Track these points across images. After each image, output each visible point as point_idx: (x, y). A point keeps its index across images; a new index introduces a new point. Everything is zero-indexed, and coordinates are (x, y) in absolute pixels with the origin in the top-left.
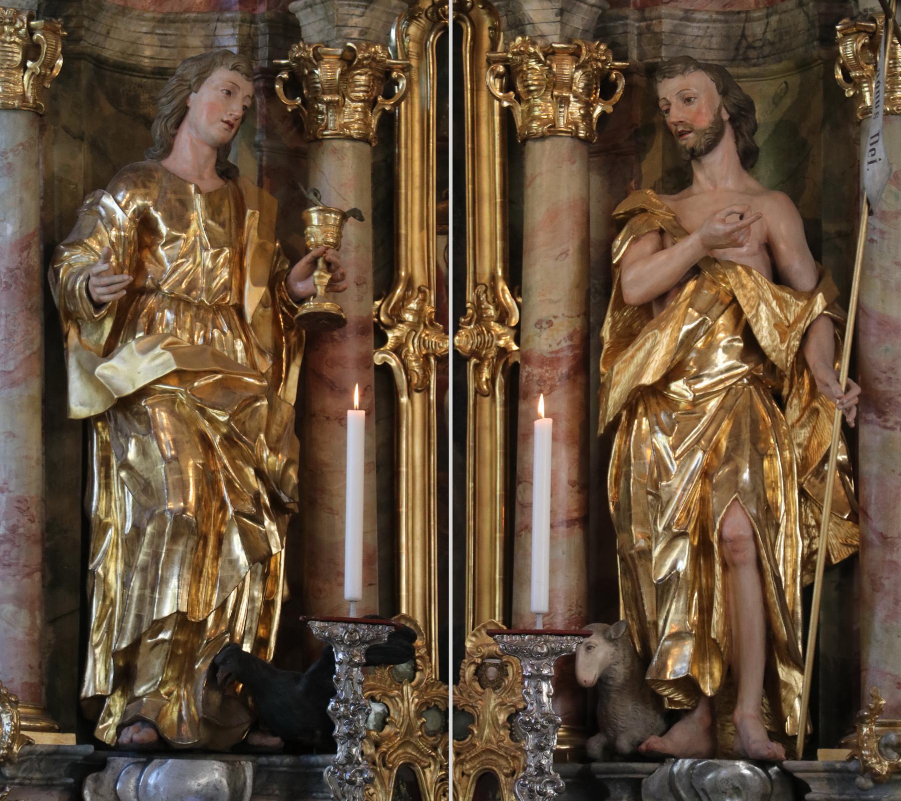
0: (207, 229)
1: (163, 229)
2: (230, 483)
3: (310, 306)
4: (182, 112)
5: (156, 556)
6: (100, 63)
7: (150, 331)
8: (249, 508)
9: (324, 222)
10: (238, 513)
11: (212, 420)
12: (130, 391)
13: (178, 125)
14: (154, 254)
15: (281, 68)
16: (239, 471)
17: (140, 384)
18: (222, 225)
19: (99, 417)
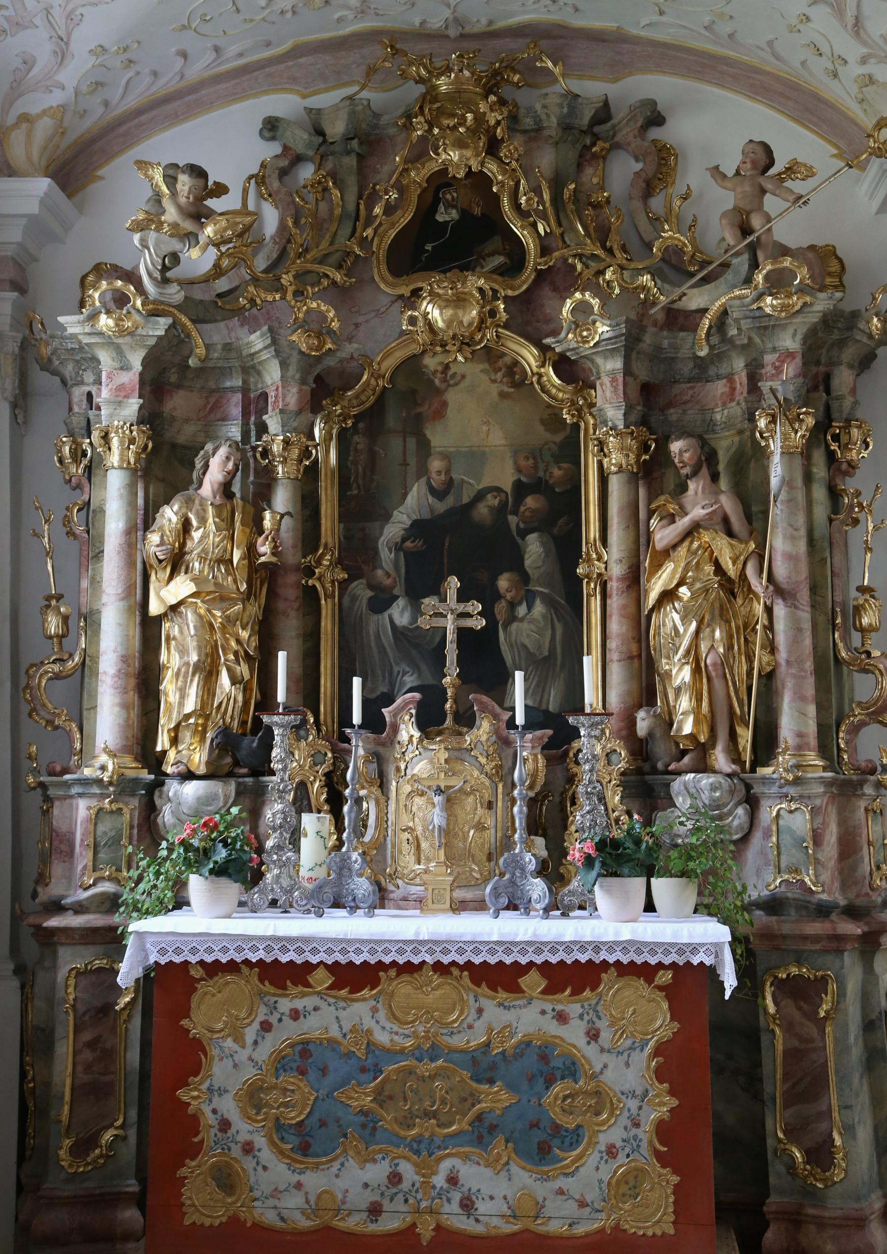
0: (215, 522)
1: (195, 523)
2: (222, 646)
3: (263, 559)
4: (206, 467)
5: (185, 682)
6: (174, 446)
7: (186, 573)
8: (232, 657)
9: (273, 518)
10: (226, 660)
11: (214, 616)
12: (174, 602)
13: (204, 474)
14: (190, 535)
15: (258, 446)
16: (227, 640)
17: (179, 599)
18: (223, 520)
19: (165, 614)
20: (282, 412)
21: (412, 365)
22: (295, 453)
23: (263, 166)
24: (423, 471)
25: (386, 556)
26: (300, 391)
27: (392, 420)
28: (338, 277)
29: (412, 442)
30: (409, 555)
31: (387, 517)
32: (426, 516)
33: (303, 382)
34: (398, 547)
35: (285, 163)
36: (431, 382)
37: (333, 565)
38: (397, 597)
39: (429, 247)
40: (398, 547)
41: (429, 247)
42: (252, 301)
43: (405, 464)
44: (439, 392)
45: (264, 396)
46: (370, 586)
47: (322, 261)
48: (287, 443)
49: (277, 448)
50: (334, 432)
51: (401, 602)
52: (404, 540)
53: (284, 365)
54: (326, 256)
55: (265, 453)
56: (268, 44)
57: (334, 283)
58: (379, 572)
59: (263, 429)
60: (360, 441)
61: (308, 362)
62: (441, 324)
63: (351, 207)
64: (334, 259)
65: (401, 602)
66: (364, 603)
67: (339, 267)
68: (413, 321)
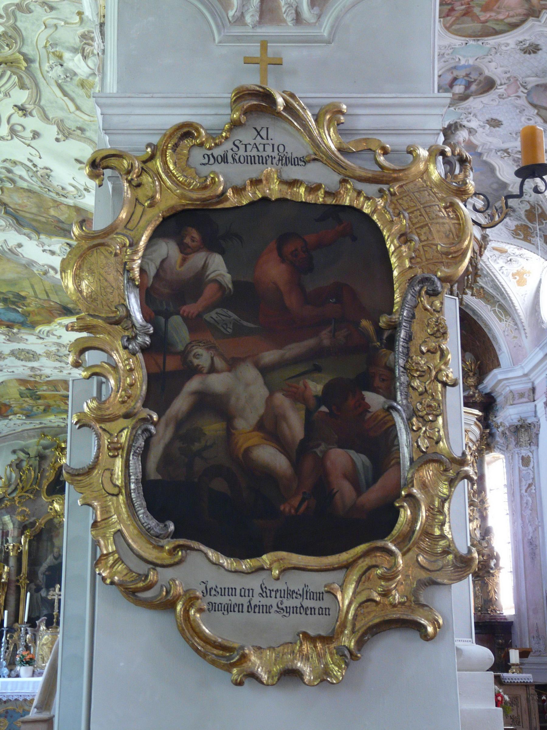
20: (13, 537)
21: (50, 521)
22: (16, 548)
23: (12, 462)
24: (52, 552)
25: (40, 576)
26: (18, 531)
27: (45, 537)
28: (32, 497)
29: (49, 544)
30: (47, 576)
31: (40, 565)
32: (52, 564)
33: (19, 528)
34: (44, 574)
35: (17, 462)
36: (55, 526)
37: (25, 579)
38: (42, 588)
39: (58, 488)
40: (44, 574)
41: (58, 488)
42: (6, 505)
43: (47, 550)
44: (57, 529)
45: (8, 531)
46: (35, 585)
47: (26, 492)
48: (14, 546)
49: (10, 548)
50: (28, 540)
51: (44, 590)
52: (46, 571)
53: (14, 524)
54: (28, 490)
55: (8, 548)
56: (14, 430)
57: (30, 498)
58: (38, 581)
59: (7, 541)
60: (35, 543)
61: (20, 523)
62: (59, 510)
63: (36, 476)
64: (30, 491)
65: (44, 590)
66: (33, 589)
67: (31, 493)
68: (51, 509)
